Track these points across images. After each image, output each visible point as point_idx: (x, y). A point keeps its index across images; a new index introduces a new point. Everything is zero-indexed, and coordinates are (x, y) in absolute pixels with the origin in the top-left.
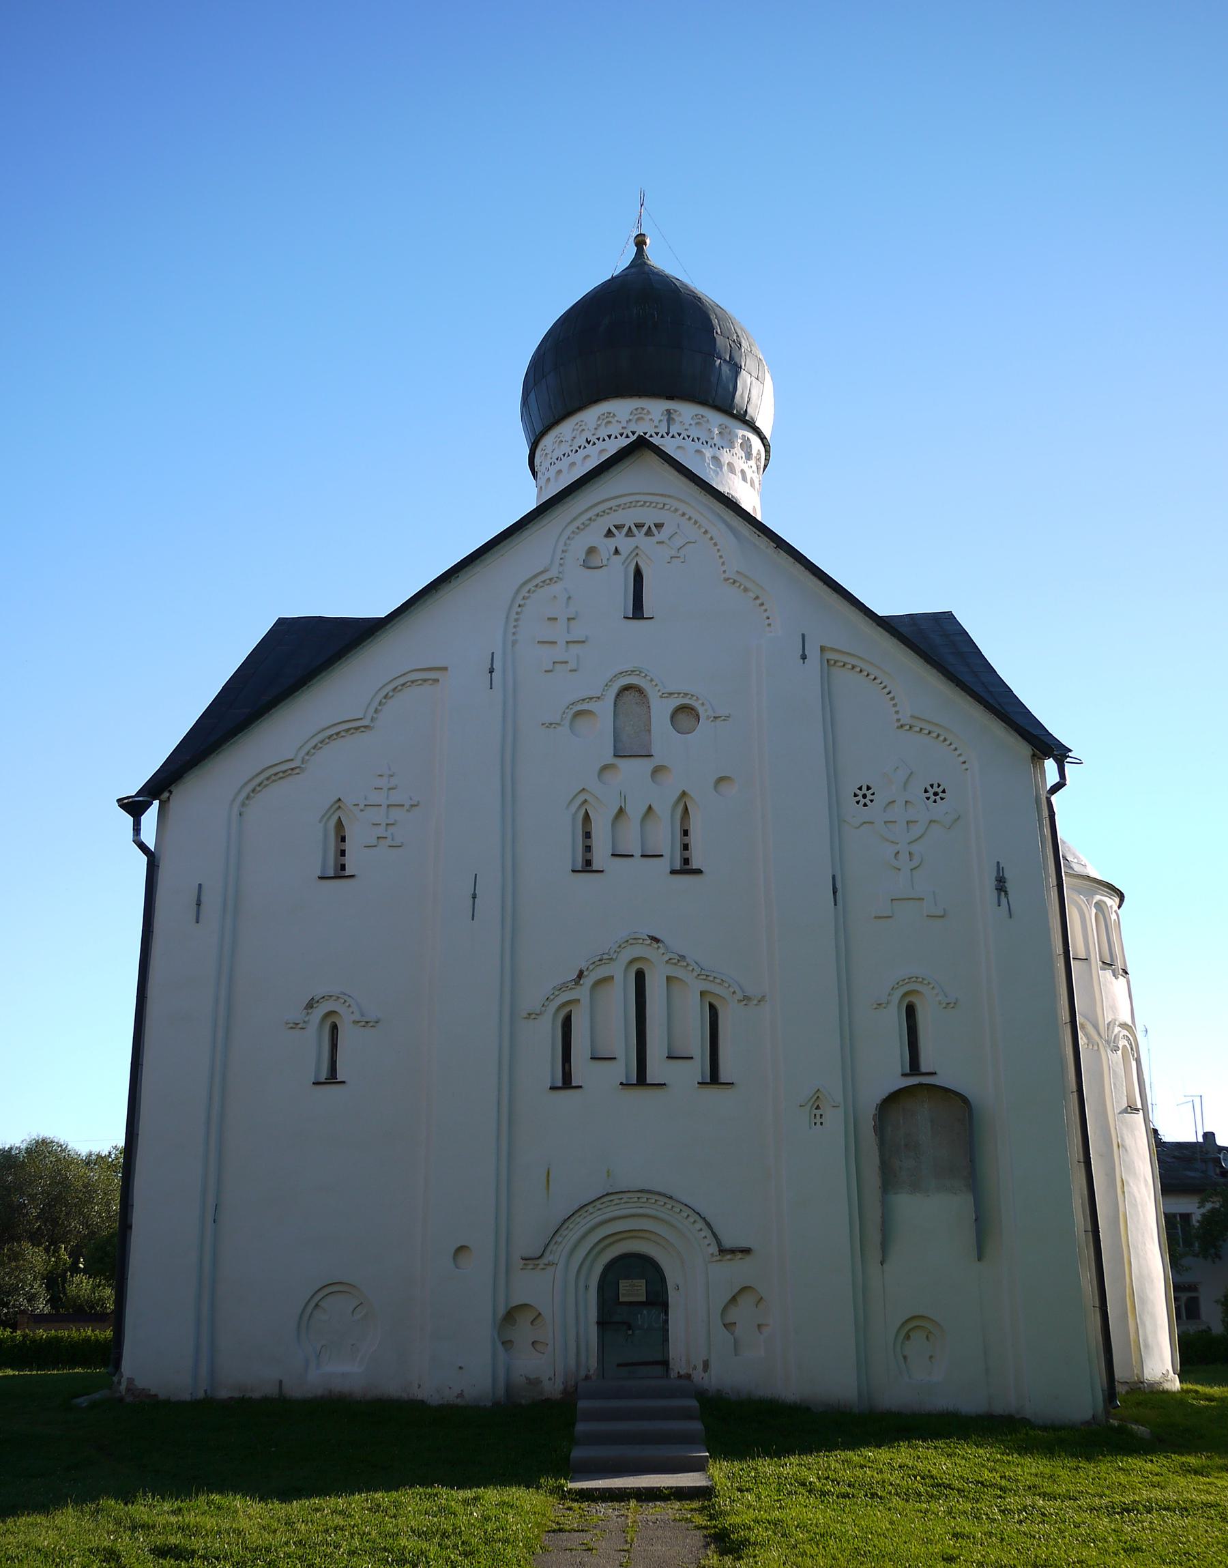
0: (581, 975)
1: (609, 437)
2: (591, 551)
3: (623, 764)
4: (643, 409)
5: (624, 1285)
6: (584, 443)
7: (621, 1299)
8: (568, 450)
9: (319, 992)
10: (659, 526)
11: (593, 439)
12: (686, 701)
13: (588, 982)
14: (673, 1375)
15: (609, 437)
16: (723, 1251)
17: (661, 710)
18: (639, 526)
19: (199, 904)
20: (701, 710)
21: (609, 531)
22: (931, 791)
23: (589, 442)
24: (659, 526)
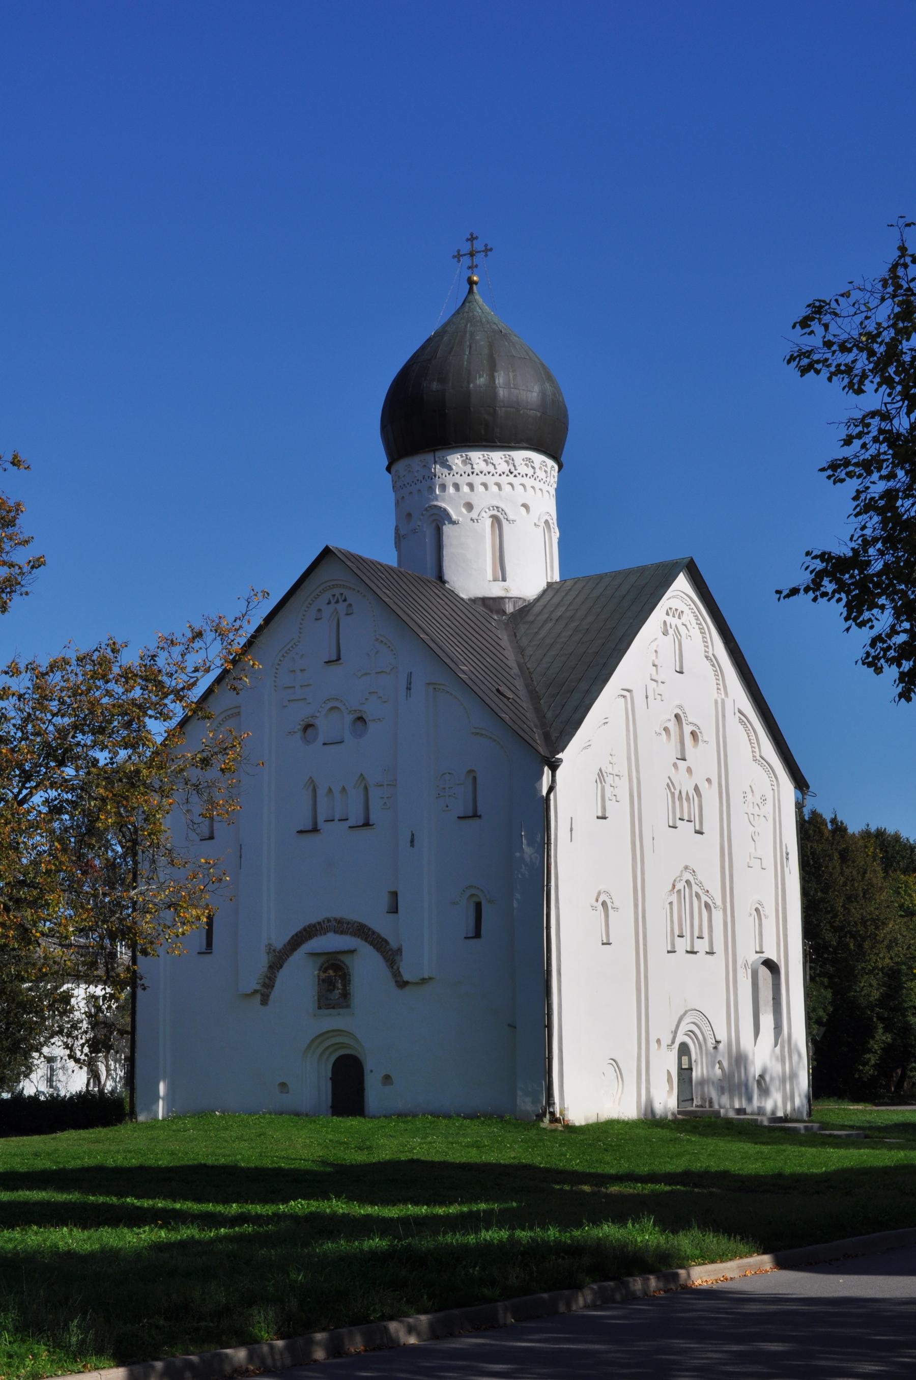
0: (674, 886)
1: (526, 475)
2: (665, 622)
3: (680, 763)
4: (544, 462)
5: (683, 1058)
6: (507, 472)
7: (683, 1067)
8: (493, 471)
9: (602, 887)
10: (682, 612)
11: (515, 473)
12: (694, 728)
13: (676, 890)
14: (694, 1105)
15: (526, 475)
16: (716, 1041)
17: (687, 729)
18: (676, 610)
19: (571, 831)
20: (699, 734)
21: (667, 611)
22: (763, 798)
23: (511, 473)
24: (682, 612)
